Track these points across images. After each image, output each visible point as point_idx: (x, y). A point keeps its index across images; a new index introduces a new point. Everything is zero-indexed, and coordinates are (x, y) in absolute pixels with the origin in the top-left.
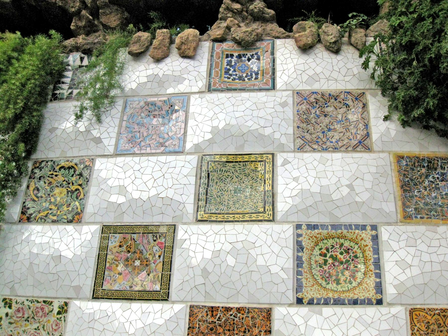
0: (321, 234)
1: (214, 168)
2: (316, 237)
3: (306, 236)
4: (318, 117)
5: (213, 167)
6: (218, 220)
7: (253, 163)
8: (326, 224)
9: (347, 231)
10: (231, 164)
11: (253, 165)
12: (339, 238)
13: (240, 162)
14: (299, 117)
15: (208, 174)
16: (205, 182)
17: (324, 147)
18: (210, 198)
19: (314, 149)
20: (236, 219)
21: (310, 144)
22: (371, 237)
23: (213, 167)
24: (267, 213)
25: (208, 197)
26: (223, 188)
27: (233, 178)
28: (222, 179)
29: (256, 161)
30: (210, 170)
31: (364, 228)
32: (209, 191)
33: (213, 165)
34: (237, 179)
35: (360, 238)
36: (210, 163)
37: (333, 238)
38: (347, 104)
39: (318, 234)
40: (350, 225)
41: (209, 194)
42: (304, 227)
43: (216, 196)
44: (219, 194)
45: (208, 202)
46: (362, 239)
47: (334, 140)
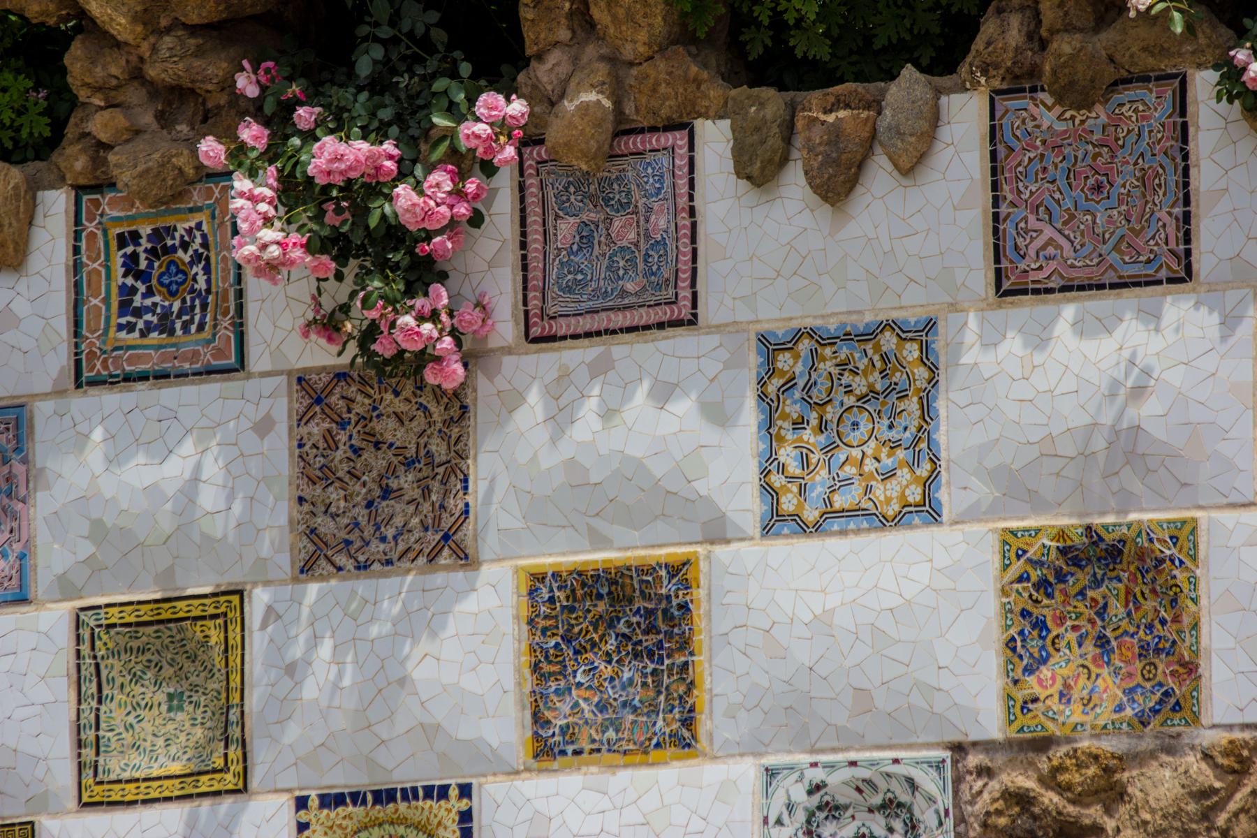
0: (351, 819)
1: (110, 645)
2: (340, 826)
3: (318, 828)
4: (357, 451)
5: (105, 644)
6: (127, 799)
7: (199, 623)
8: (363, 790)
9: (406, 804)
10: (150, 630)
11: (198, 629)
12: (392, 823)
13: (169, 621)
14: (302, 464)
15: (97, 666)
16: (89, 692)
17: (362, 558)
18: (110, 734)
19: (340, 569)
20: (167, 794)
21: (330, 553)
22: (457, 818)
23: (105, 644)
24: (232, 769)
25: (101, 733)
26: (138, 698)
27: (161, 668)
28: (135, 675)
29: (203, 618)
30: (99, 654)
31: (443, 792)
32: (102, 717)
33: (105, 637)
34: (171, 671)
35: (436, 821)
36: (97, 630)
37: (380, 825)
38: (426, 408)
39: (345, 818)
40: (415, 790)
41: (103, 725)
42: (314, 803)
43: (122, 730)
44: (131, 719)
45: (102, 749)
46: (439, 823)
47: (390, 533)
